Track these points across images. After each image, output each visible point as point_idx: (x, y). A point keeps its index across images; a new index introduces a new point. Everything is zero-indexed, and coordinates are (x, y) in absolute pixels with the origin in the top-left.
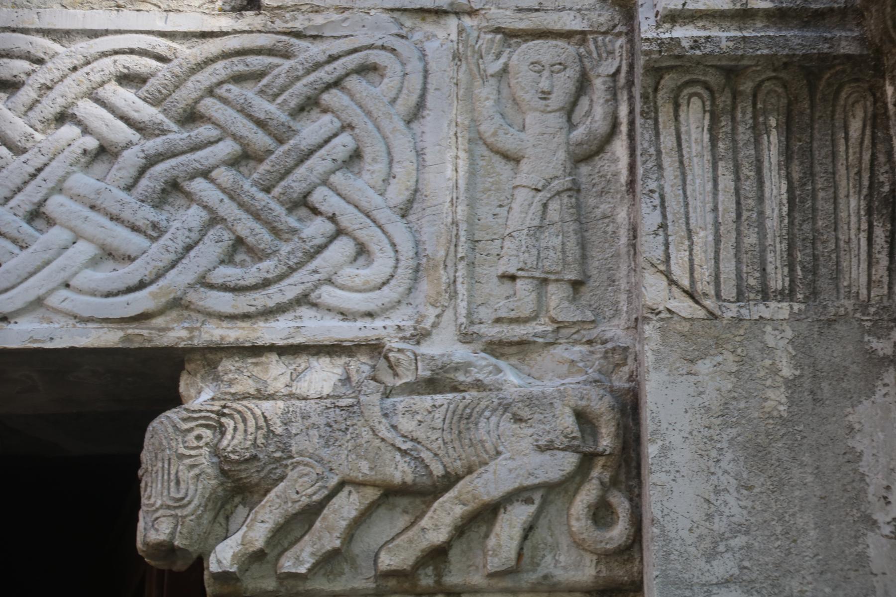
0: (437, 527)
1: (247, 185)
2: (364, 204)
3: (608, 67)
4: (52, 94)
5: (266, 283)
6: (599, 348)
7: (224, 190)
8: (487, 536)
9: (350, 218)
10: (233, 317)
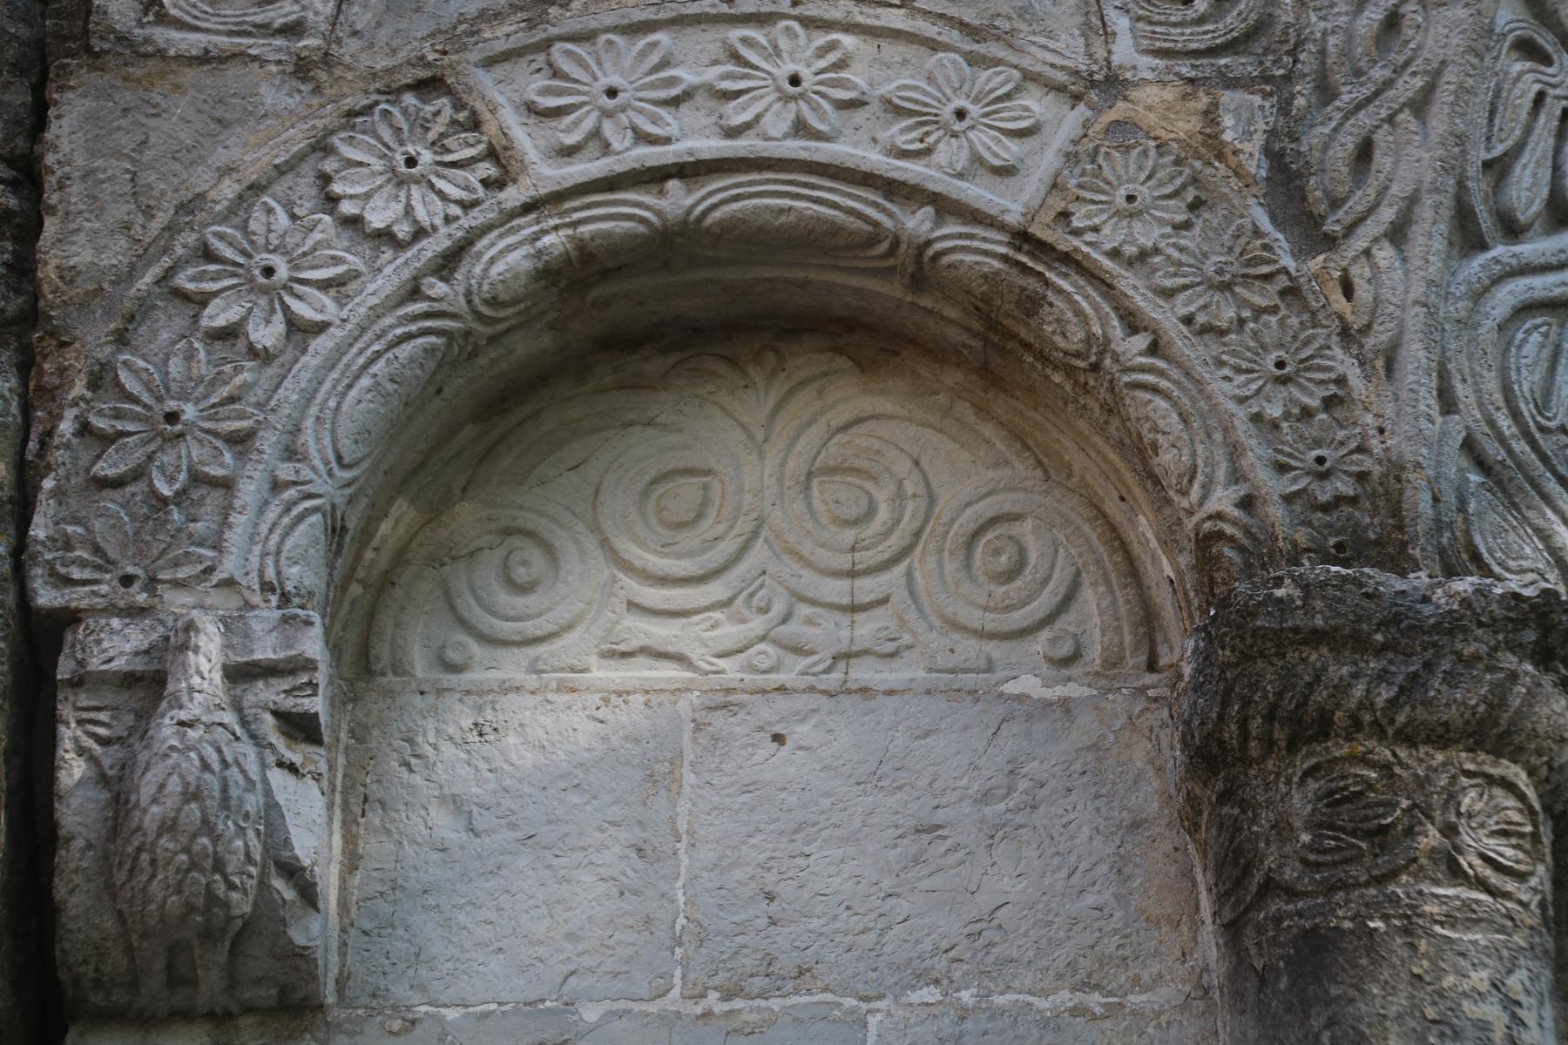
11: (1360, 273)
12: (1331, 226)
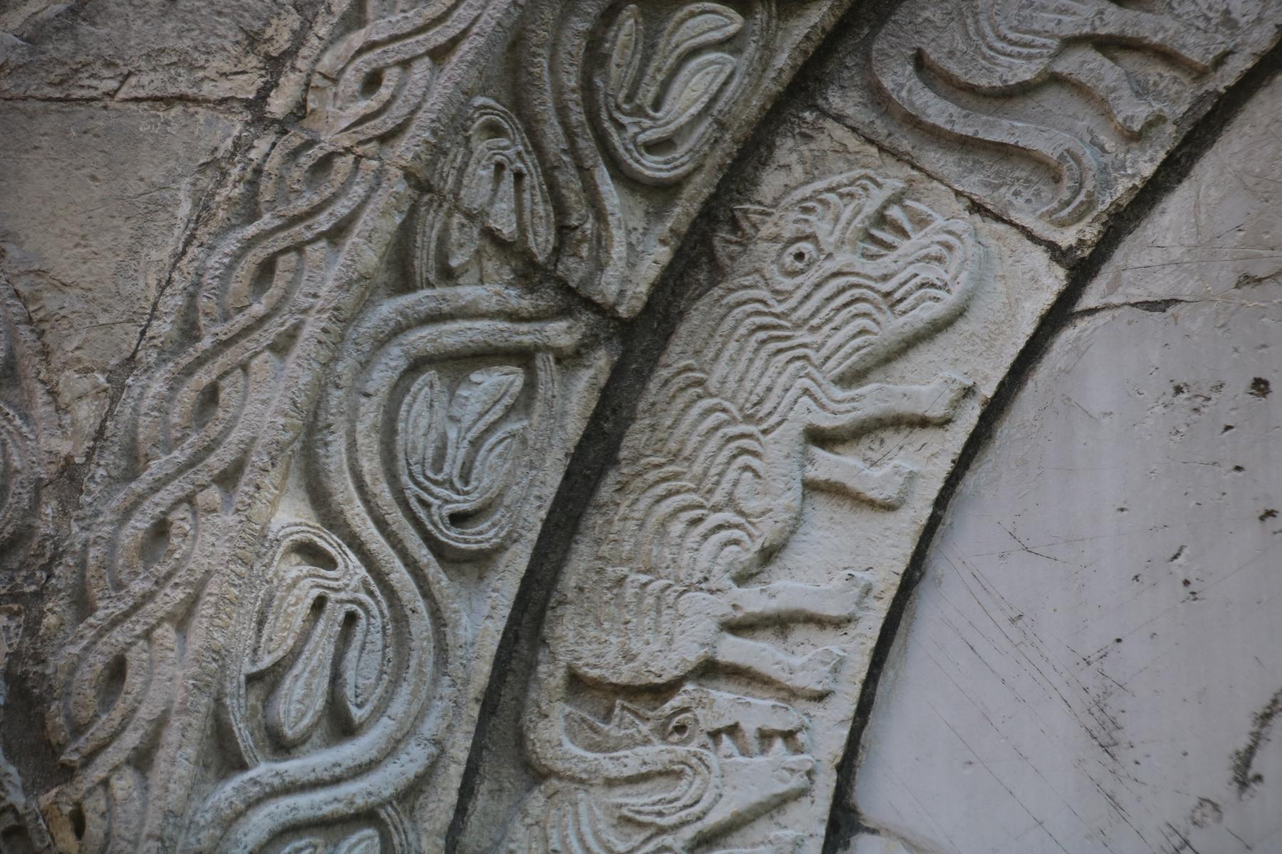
11: (94, 806)
12: (70, 756)
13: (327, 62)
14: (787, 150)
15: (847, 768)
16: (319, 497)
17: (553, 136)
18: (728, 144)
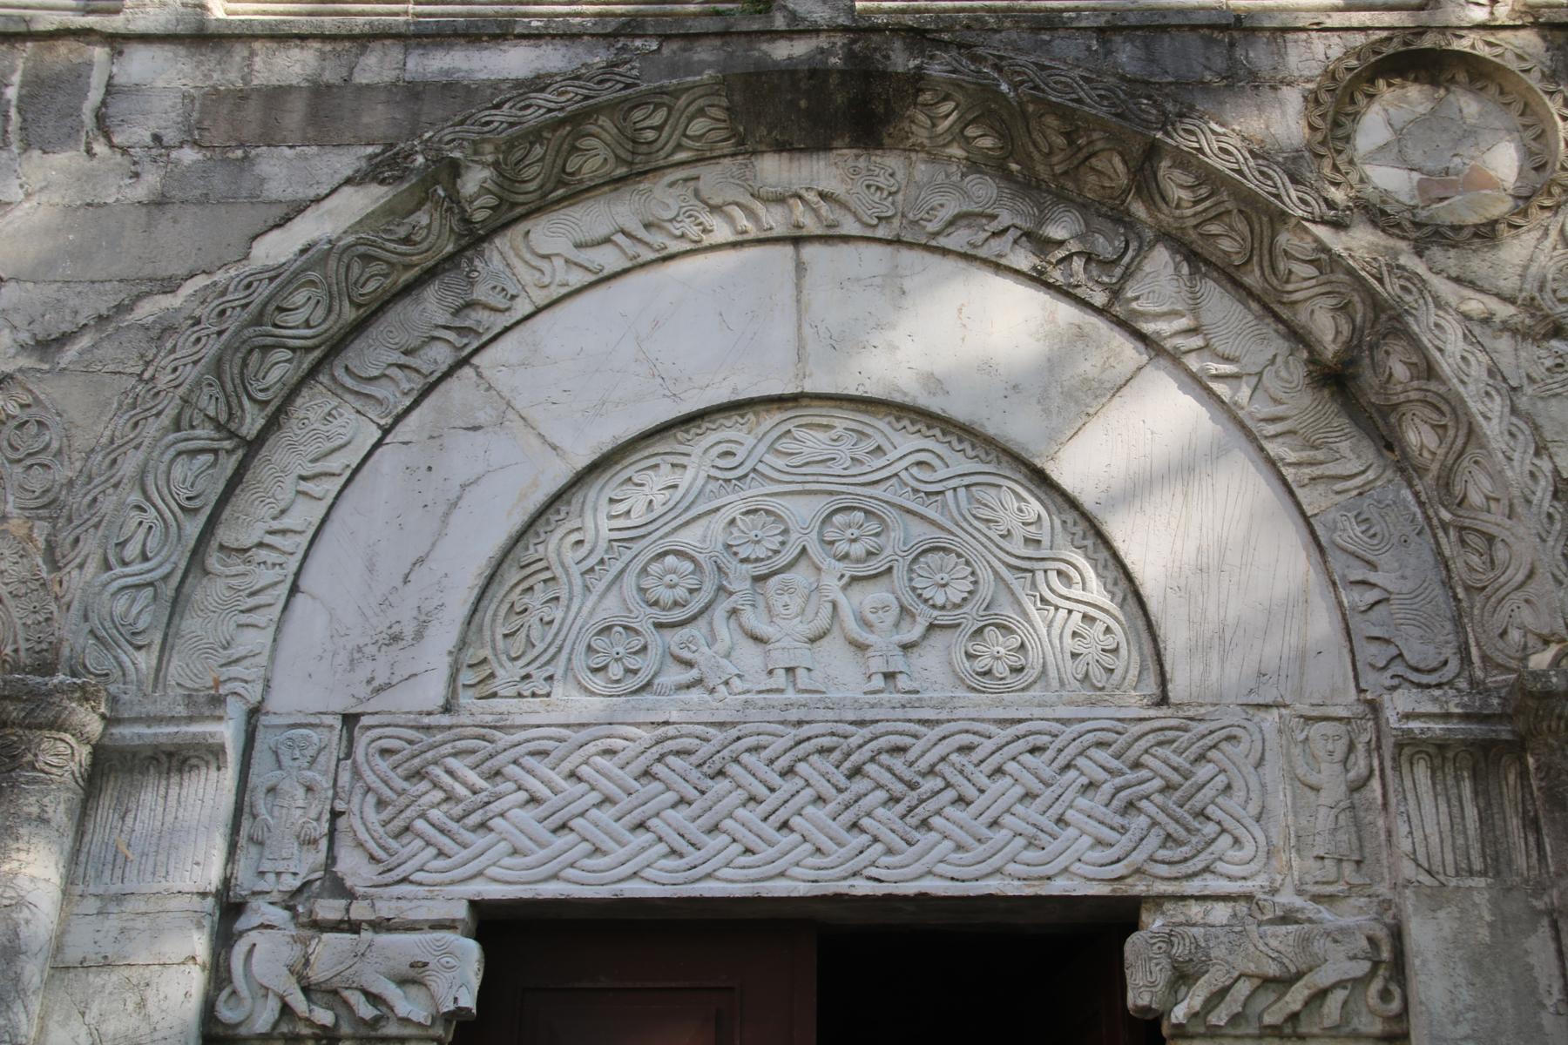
0: (1294, 1002)
1: (1170, 804)
2: (1236, 815)
3: (1365, 738)
4: (1063, 754)
5: (1186, 860)
6: (1374, 899)
7: (1158, 807)
8: (1321, 1006)
9: (1229, 823)
10: (1169, 879)
11: (66, 578)
12: (60, 564)
13: (163, 363)
14: (305, 392)
15: (297, 574)
16: (144, 492)
17: (229, 387)
18: (286, 390)
